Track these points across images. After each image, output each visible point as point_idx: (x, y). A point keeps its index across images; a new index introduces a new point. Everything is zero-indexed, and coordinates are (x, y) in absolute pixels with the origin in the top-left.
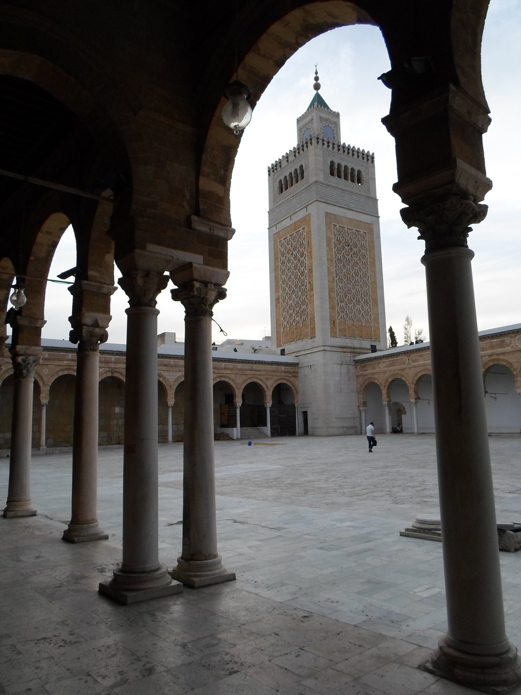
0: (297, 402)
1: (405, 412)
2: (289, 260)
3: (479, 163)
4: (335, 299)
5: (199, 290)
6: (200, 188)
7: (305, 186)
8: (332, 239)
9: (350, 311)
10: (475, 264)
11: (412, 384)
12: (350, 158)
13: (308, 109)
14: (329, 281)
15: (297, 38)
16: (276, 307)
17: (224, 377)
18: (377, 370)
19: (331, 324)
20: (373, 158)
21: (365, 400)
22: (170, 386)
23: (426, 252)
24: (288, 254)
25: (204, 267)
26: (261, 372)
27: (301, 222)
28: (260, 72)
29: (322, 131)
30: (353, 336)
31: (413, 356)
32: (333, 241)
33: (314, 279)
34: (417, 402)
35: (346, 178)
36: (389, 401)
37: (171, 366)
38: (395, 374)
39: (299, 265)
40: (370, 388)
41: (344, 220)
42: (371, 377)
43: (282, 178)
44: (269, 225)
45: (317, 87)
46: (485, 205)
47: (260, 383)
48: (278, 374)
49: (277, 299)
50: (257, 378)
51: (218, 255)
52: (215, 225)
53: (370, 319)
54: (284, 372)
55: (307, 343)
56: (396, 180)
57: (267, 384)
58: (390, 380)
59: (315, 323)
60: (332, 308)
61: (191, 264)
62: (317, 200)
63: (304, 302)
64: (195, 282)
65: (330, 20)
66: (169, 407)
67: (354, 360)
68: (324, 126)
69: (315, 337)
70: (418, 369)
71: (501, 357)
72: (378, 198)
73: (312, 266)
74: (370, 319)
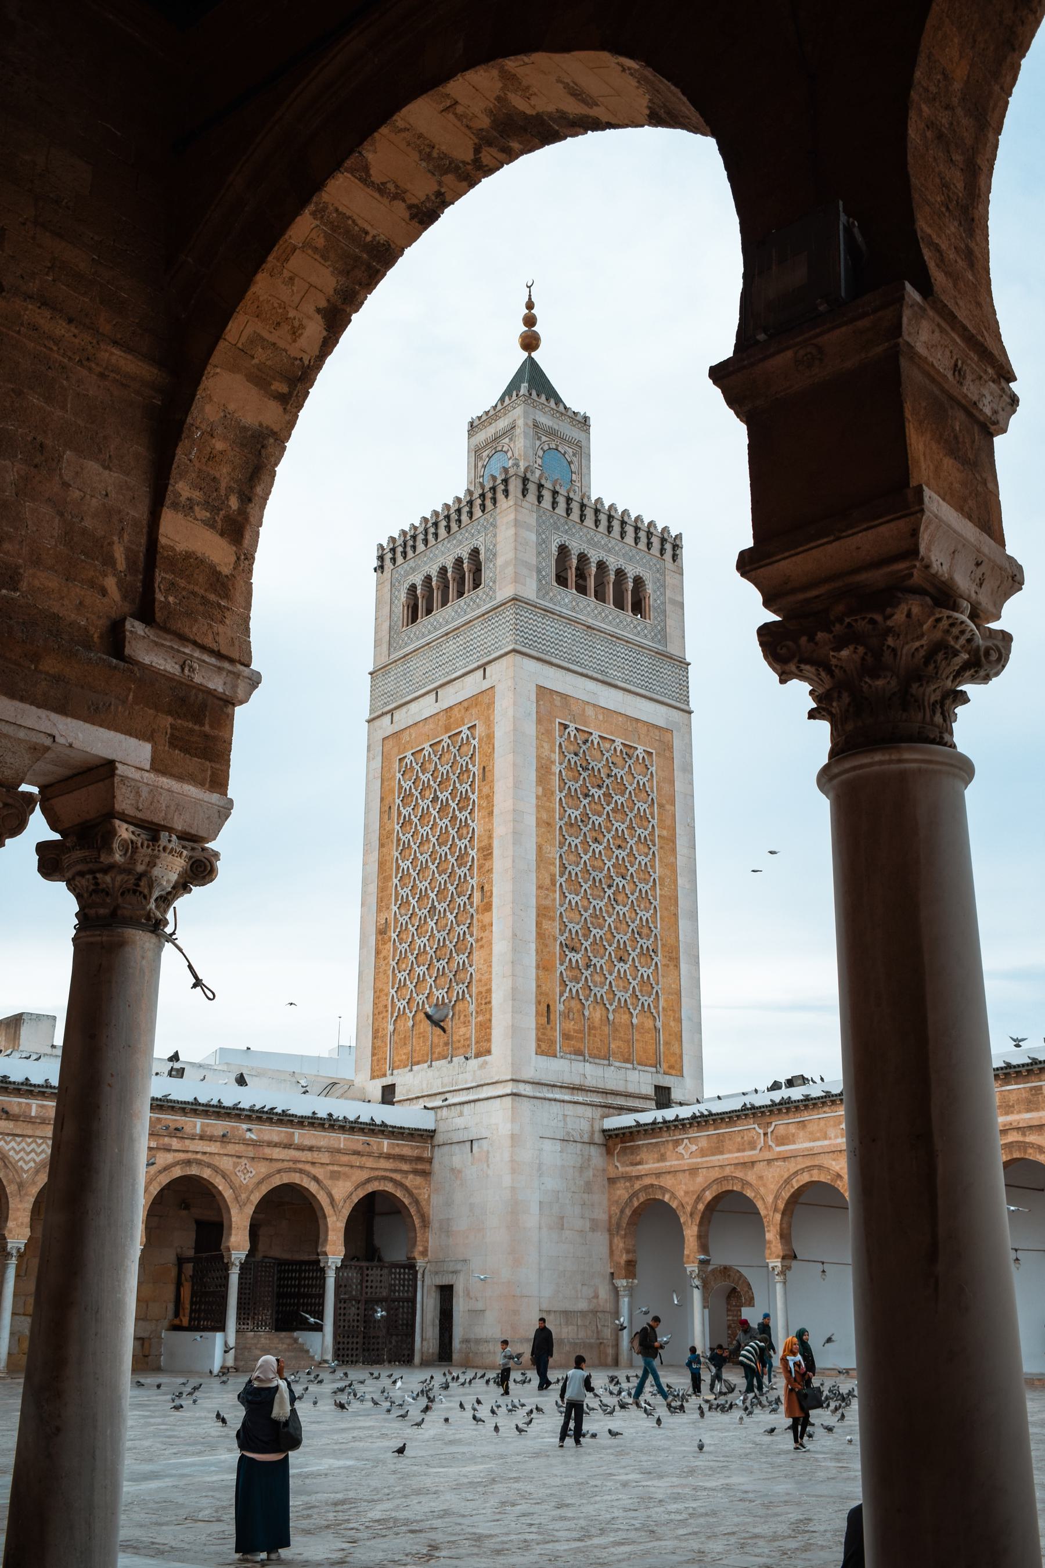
0: (424, 1253)
1: (752, 1298)
3: (985, 511)
4: (555, 939)
5: (130, 848)
6: (163, 540)
7: (483, 609)
9: (597, 978)
10: (975, 798)
11: (776, 1210)
12: (613, 542)
13: (502, 399)
14: (539, 887)
15: (477, 150)
16: (378, 952)
18: (671, 1163)
20: (676, 547)
21: (630, 1257)
22: (21, 1185)
23: (833, 754)
24: (423, 798)
25: (150, 777)
26: (315, 1154)
27: (467, 709)
28: (367, 233)
29: (539, 461)
30: (604, 1056)
31: (780, 1124)
32: (556, 768)
33: (496, 876)
34: (789, 1268)
35: (600, 596)
36: (703, 1263)
38: (725, 1178)
39: (453, 832)
40: (647, 1219)
41: (590, 712)
42: (652, 1185)
43: (418, 579)
45: (530, 342)
46: (1002, 631)
47: (313, 1187)
48: (370, 1163)
50: (301, 1171)
51: (198, 733)
52: (197, 654)
53: (656, 1007)
54: (388, 1157)
56: (748, 542)
57: (333, 1192)
58: (709, 1196)
59: (491, 1009)
60: (543, 966)
61: (109, 765)
62: (514, 651)
63: (460, 945)
64: (117, 822)
65: (574, 108)
66: (9, 1255)
67: (604, 1131)
68: (546, 447)
69: (489, 1052)
70: (793, 1166)
71: (1032, 1138)
72: (688, 660)
73: (490, 837)
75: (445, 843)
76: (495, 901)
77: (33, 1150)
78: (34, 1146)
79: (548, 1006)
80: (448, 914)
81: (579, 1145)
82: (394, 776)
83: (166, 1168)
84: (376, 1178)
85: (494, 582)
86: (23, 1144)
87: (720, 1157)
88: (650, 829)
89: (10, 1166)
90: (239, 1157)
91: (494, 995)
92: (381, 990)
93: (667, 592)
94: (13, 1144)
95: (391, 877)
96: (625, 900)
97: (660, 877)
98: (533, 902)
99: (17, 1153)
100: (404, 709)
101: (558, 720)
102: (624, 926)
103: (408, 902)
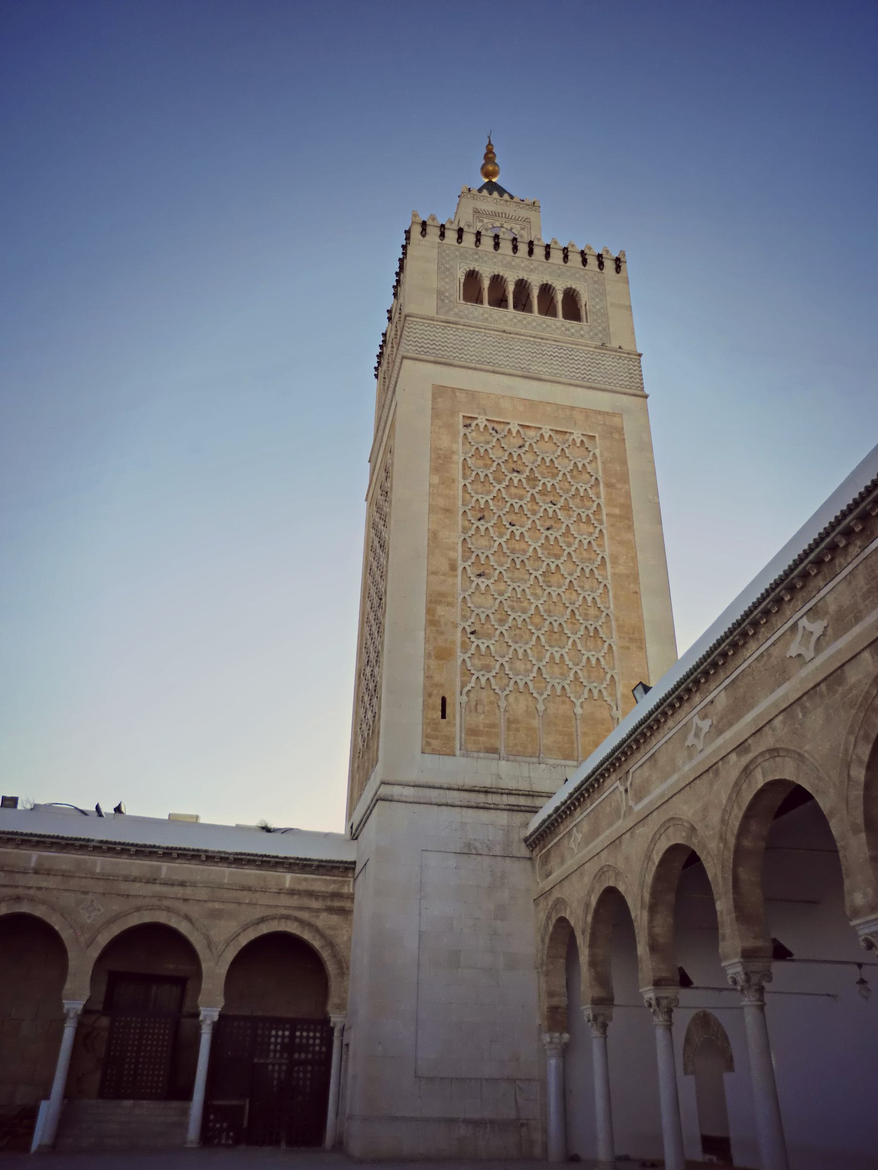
0: (341, 1007)
4: (456, 626)
8: (453, 453)
17: (32, 900)
19: (426, 706)
26: (189, 890)
47: (183, 927)
48: (264, 899)
50: (168, 909)
53: (613, 695)
54: (292, 892)
57: (212, 933)
74: (613, 695)
79: (444, 700)
81: (487, 861)
84: (273, 918)
88: (595, 508)
90: (86, 893)
93: (608, 298)
96: (561, 581)
97: (611, 556)
101: (461, 414)
102: (560, 608)
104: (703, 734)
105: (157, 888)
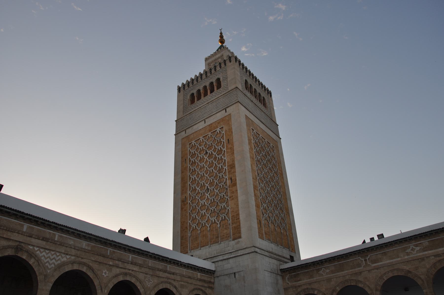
2: (202, 160)
11: (376, 290)
13: (218, 50)
14: (253, 178)
20: (271, 93)
22: (46, 276)
24: (200, 154)
27: (219, 123)
32: (253, 142)
37: (54, 242)
42: (307, 288)
43: (195, 91)
44: (176, 132)
45: (222, 41)
49: (184, 202)
50: (170, 283)
54: (200, 280)
55: (231, 245)
58: (338, 289)
67: (281, 270)
69: (240, 237)
73: (233, 161)
75: (212, 167)
76: (238, 182)
77: (54, 258)
78: (55, 256)
80: (215, 190)
82: (187, 150)
83: (116, 276)
85: (227, 85)
86: (49, 255)
87: (343, 272)
89: (41, 265)
90: (147, 274)
91: (240, 216)
92: (184, 222)
94: (44, 253)
95: (187, 182)
98: (252, 183)
99: (46, 259)
100: (191, 128)
103: (196, 190)
104: (416, 250)
105: (166, 275)
